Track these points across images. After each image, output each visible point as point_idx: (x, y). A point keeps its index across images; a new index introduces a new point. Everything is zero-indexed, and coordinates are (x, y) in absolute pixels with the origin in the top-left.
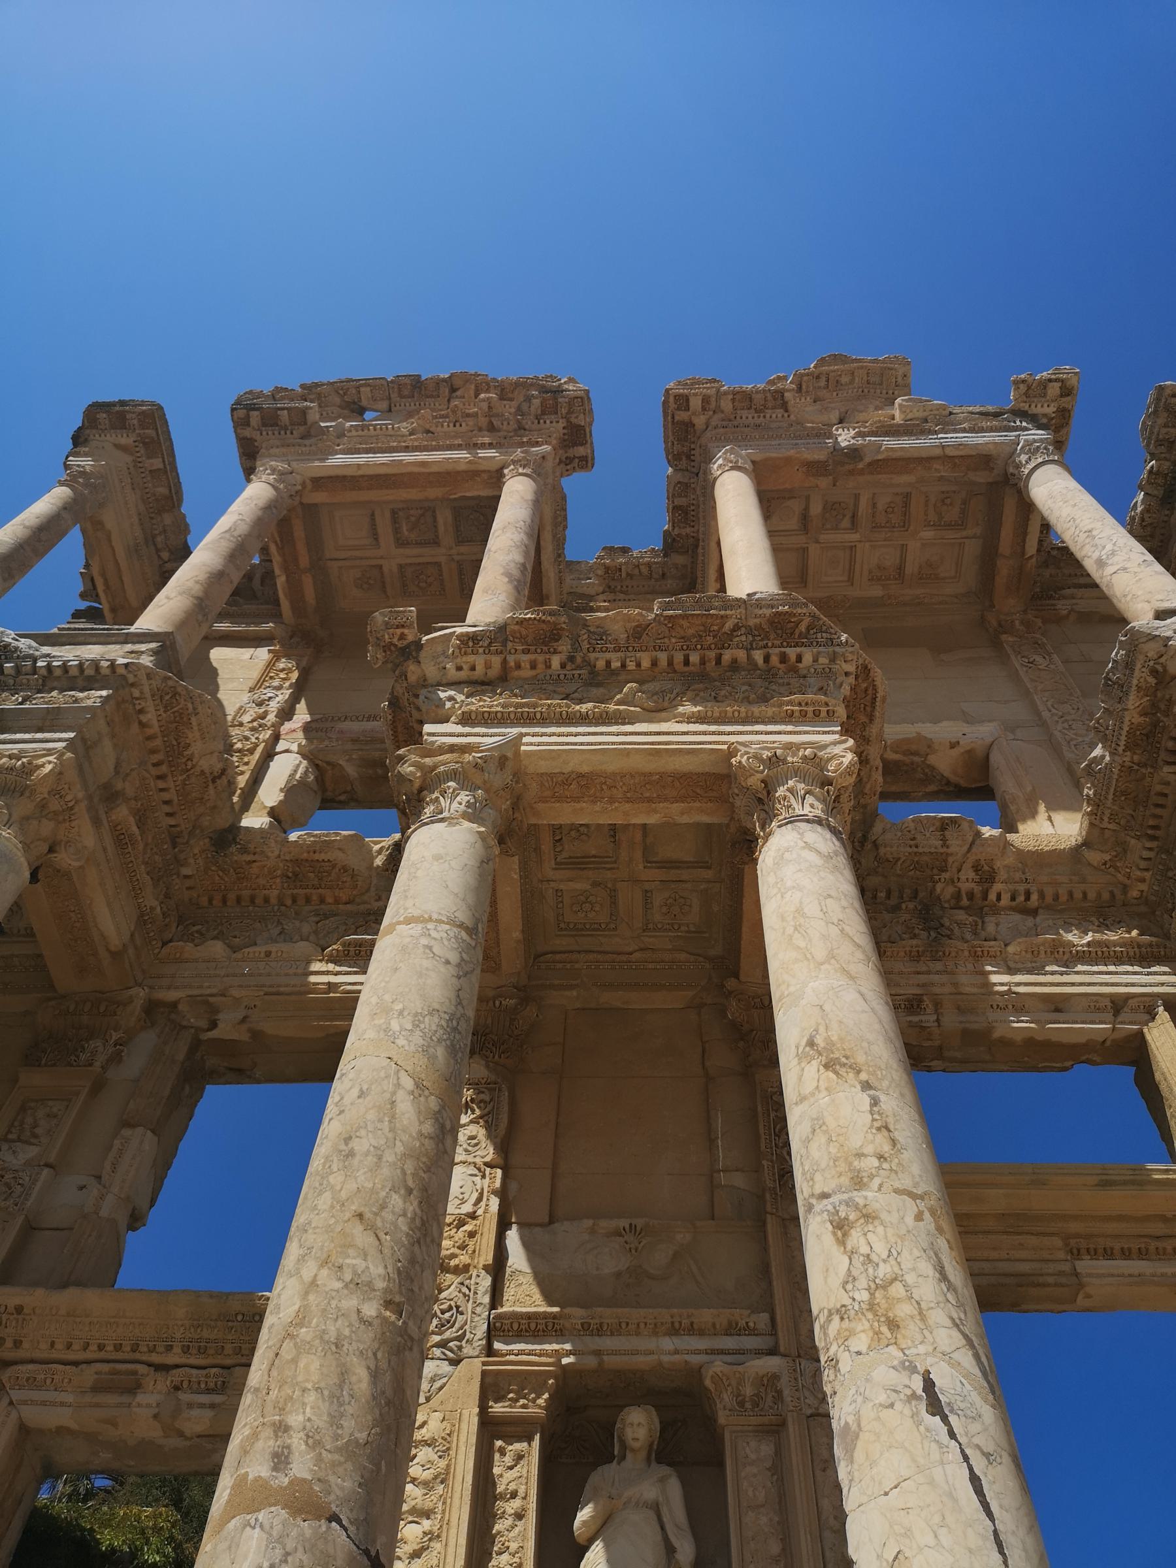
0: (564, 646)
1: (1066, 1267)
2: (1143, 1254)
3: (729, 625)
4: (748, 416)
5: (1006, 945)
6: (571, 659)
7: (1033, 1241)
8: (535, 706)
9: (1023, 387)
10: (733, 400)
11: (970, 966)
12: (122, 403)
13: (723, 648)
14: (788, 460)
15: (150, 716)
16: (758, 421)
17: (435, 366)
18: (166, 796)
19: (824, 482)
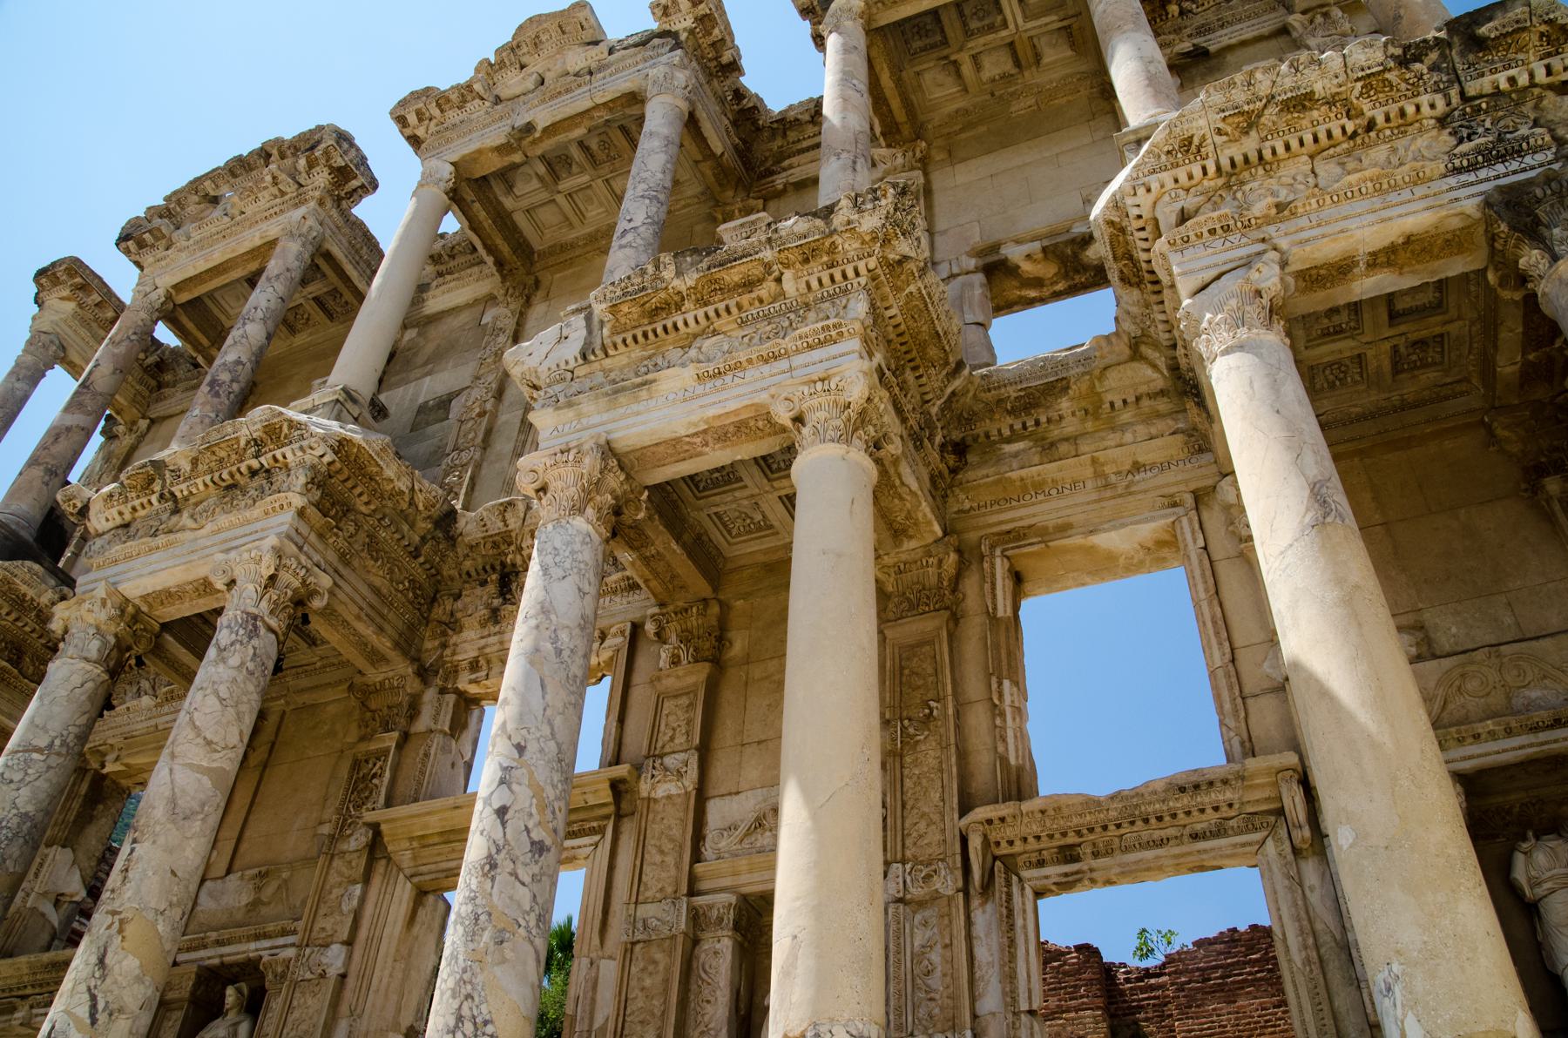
0: (157, 487)
3: (243, 443)
6: (162, 496)
9: (659, 12)
14: (480, 152)
16: (461, 117)
17: (246, 146)
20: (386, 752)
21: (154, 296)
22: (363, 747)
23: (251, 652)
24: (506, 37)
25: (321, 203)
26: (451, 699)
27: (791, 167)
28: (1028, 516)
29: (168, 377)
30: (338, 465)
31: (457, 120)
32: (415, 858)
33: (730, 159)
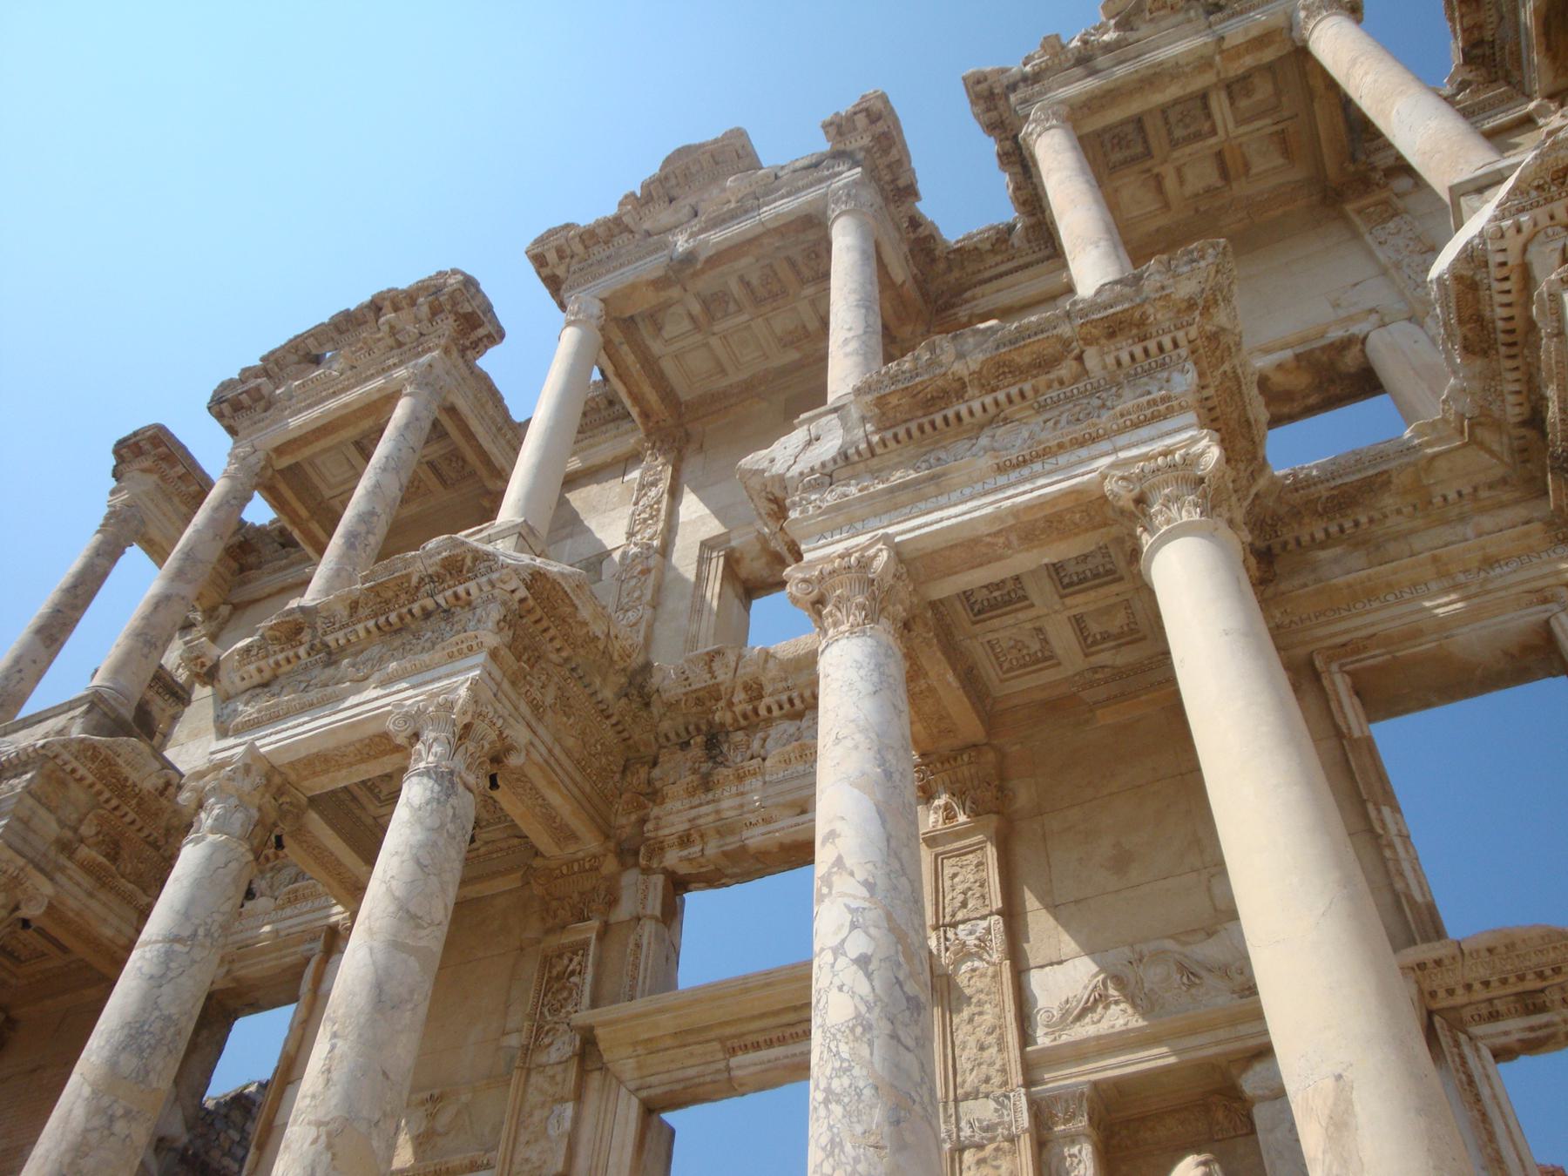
0: (306, 636)
1: (721, 1065)
2: (782, 1041)
3: (415, 580)
4: (599, 252)
5: (764, 760)
6: (312, 647)
7: (698, 1049)
8: (277, 705)
9: (833, 130)
10: (582, 240)
11: (734, 790)
12: (135, 434)
13: (414, 601)
14: (633, 287)
15: (82, 771)
18: (127, 819)
19: (675, 292)
20: (584, 945)
21: (253, 459)
22: (555, 941)
23: (450, 812)
24: (653, 169)
25: (447, 351)
26: (658, 880)
27: (974, 298)
28: (1365, 626)
29: (252, 559)
30: (531, 602)
31: (604, 255)
32: (640, 1067)
33: (911, 290)
